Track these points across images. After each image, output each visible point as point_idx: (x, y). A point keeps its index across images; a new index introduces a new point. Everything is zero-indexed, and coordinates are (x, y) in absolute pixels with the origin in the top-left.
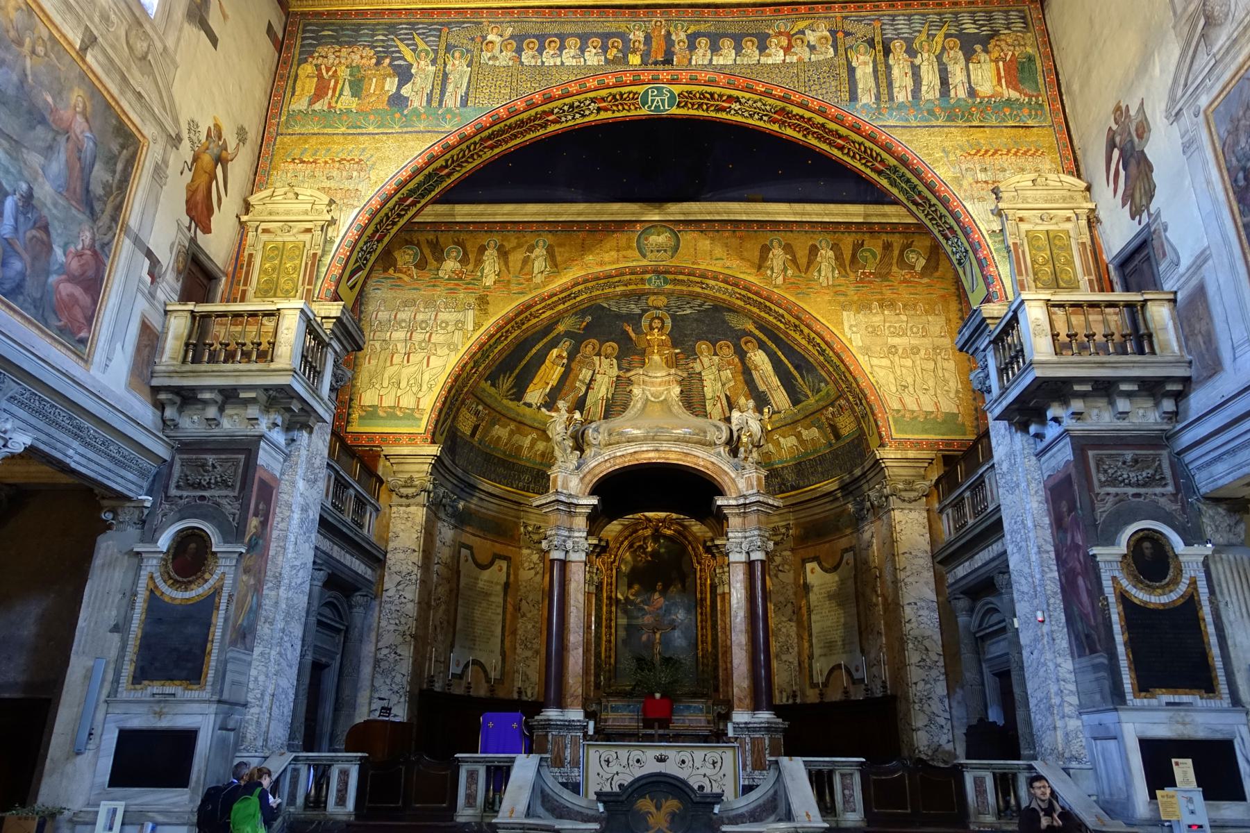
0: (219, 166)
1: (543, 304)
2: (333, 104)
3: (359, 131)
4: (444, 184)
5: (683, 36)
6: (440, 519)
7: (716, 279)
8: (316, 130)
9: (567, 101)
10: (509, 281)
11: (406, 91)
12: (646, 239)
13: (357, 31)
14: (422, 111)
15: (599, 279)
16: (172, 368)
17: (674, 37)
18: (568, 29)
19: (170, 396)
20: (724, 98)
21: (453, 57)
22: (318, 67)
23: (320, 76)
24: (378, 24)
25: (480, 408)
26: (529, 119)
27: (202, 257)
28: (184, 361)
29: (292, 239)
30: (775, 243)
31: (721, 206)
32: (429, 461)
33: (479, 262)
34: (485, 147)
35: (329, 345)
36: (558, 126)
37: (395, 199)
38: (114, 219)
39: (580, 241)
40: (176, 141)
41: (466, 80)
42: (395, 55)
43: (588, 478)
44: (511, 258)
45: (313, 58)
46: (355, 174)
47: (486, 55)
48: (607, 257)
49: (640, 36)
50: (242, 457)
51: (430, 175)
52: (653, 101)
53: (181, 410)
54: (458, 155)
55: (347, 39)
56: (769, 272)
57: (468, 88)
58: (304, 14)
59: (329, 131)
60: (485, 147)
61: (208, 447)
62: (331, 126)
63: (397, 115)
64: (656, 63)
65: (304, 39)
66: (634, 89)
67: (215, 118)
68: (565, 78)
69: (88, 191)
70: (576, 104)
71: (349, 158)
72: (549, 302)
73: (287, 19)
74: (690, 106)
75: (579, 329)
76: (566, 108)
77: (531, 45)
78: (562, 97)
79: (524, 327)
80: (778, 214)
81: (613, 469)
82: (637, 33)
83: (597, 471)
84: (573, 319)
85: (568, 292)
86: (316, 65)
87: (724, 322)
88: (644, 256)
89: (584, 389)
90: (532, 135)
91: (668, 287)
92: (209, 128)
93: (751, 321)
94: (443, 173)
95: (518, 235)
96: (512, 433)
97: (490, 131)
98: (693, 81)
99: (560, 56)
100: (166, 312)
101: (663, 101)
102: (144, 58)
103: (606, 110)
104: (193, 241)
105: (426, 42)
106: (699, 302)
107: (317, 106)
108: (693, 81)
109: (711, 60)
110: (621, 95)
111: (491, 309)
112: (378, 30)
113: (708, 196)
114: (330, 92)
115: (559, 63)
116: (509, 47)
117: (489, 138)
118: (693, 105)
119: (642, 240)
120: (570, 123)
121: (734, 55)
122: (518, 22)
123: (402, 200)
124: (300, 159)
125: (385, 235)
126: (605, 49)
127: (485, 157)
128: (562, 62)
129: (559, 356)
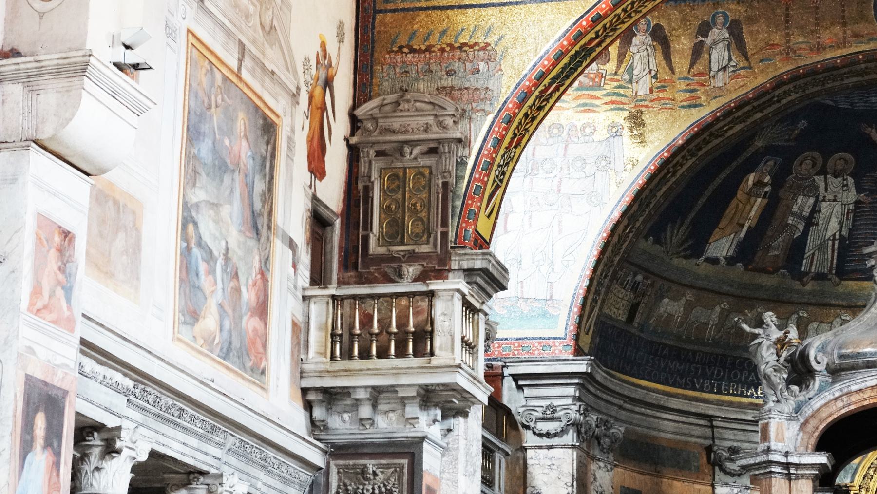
0: (328, 89)
1: (730, 119)
6: (593, 458)
16: (322, 367)
19: (320, 396)
25: (639, 278)
27: (321, 210)
28: (333, 357)
29: (414, 164)
32: (576, 381)
35: (480, 311)
37: (537, 93)
38: (269, 228)
39: (784, 10)
40: (295, 96)
43: (813, 423)
44: (675, 46)
46: (482, 66)
48: (826, 37)
50: (405, 462)
53: (329, 409)
54: (611, 22)
61: (366, 450)
67: (321, 36)
69: (253, 212)
71: (472, 41)
72: (740, 113)
75: (788, 140)
79: (700, 153)
81: (847, 410)
83: (824, 414)
85: (768, 97)
89: (801, 227)
96: (689, 307)
100: (304, 298)
102: (272, 27)
104: (315, 198)
111: (649, 137)
125: (524, 136)
129: (759, 183)
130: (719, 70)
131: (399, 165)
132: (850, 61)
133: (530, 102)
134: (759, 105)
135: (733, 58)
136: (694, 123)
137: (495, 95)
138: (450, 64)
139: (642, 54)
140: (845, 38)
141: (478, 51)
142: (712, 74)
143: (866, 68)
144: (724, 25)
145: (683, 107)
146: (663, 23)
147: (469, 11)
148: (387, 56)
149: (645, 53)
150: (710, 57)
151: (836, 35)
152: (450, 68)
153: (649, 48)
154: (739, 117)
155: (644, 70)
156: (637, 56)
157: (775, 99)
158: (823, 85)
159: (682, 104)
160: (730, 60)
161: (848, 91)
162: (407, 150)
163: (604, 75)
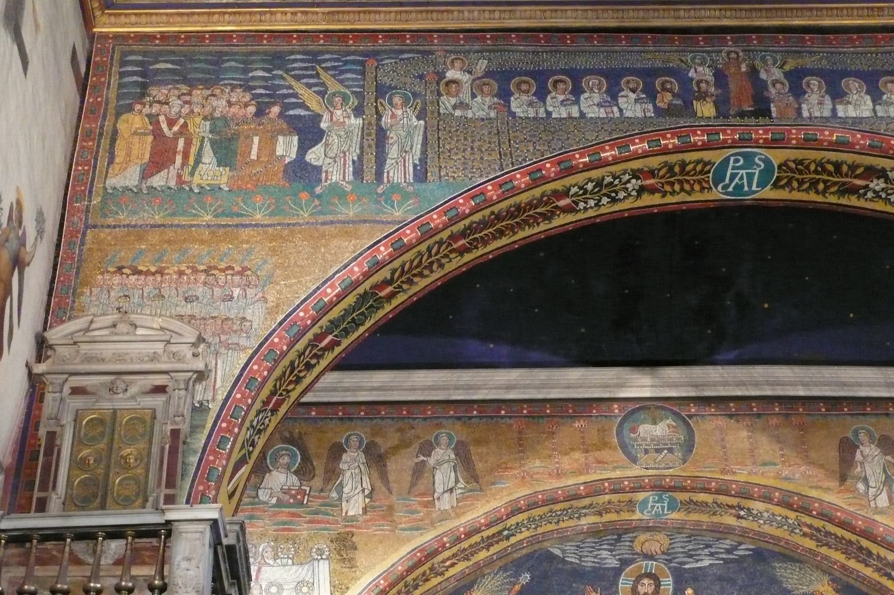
1: (455, 550)
2: (186, 178)
3: (237, 220)
4: (381, 313)
5: (777, 74)
7: (767, 499)
8: (158, 219)
9: (595, 174)
10: (391, 508)
11: (314, 156)
12: (633, 430)
13: (216, 63)
14: (349, 188)
15: (555, 501)
17: (763, 75)
18: (581, 62)
20: (859, 171)
21: (391, 103)
22: (153, 119)
23: (157, 133)
24: (253, 53)
26: (531, 205)
30: (862, 436)
31: (759, 372)
33: (332, 474)
34: (453, 251)
36: (570, 218)
37: (310, 335)
41: (418, 140)
42: (287, 102)
44: (392, 466)
45: (144, 105)
46: (237, 292)
47: (447, 102)
48: (566, 462)
49: (706, 73)
51: (364, 297)
52: (733, 177)
54: (412, 262)
55: (201, 76)
56: (861, 486)
57: (424, 152)
58: (116, 36)
59: (183, 220)
60: (453, 251)
62: (184, 213)
63: (304, 196)
64: (742, 115)
65: (122, 75)
66: (707, 155)
67: (18, 190)
68: (591, 136)
70: (609, 179)
71: (223, 265)
72: (465, 545)
73: (91, 43)
74: (795, 184)
76: (590, 186)
77: (524, 87)
78: (588, 168)
80: (860, 385)
82: (700, 69)
84: (501, 576)
86: (149, 116)
87: (774, 581)
88: (634, 460)
90: (527, 232)
91: (675, 515)
92: (12, 204)
93: (826, 579)
94: (383, 294)
95: (400, 424)
97: (467, 222)
98: (808, 143)
99: (577, 102)
101: (750, 176)
103: (652, 190)
105: (341, 82)
106: (727, 543)
107: (157, 181)
108: (808, 143)
109: (834, 110)
110: (683, 165)
111: (361, 558)
112: (253, 62)
113: (732, 355)
114: (179, 159)
115: (575, 113)
116: (485, 88)
117: (463, 234)
118: (801, 183)
119: (626, 432)
120: (591, 213)
121: (871, 104)
122: (494, 51)
123: (319, 338)
124: (129, 268)
126: (651, 94)
127: (449, 267)
128: (581, 112)
130: (444, 492)
131: (107, 405)
132: (594, 490)
133: (300, 346)
134: (488, 537)
135: (461, 480)
136: (416, 549)
137: (255, 326)
138: (190, 289)
139: (353, 471)
140: (587, 464)
141: (233, 275)
142: (436, 495)
143: (609, 502)
144: (449, 445)
145: (402, 529)
146: (378, 440)
147: (221, 231)
148: (100, 277)
149: (357, 471)
150: (434, 478)
151: (576, 460)
152: (190, 293)
153: (361, 466)
154: (465, 550)
155: (356, 488)
156: (348, 474)
157: (506, 533)
158: (557, 523)
159: (400, 526)
160: (457, 481)
161: (581, 537)
162: (122, 386)
163: (307, 492)
